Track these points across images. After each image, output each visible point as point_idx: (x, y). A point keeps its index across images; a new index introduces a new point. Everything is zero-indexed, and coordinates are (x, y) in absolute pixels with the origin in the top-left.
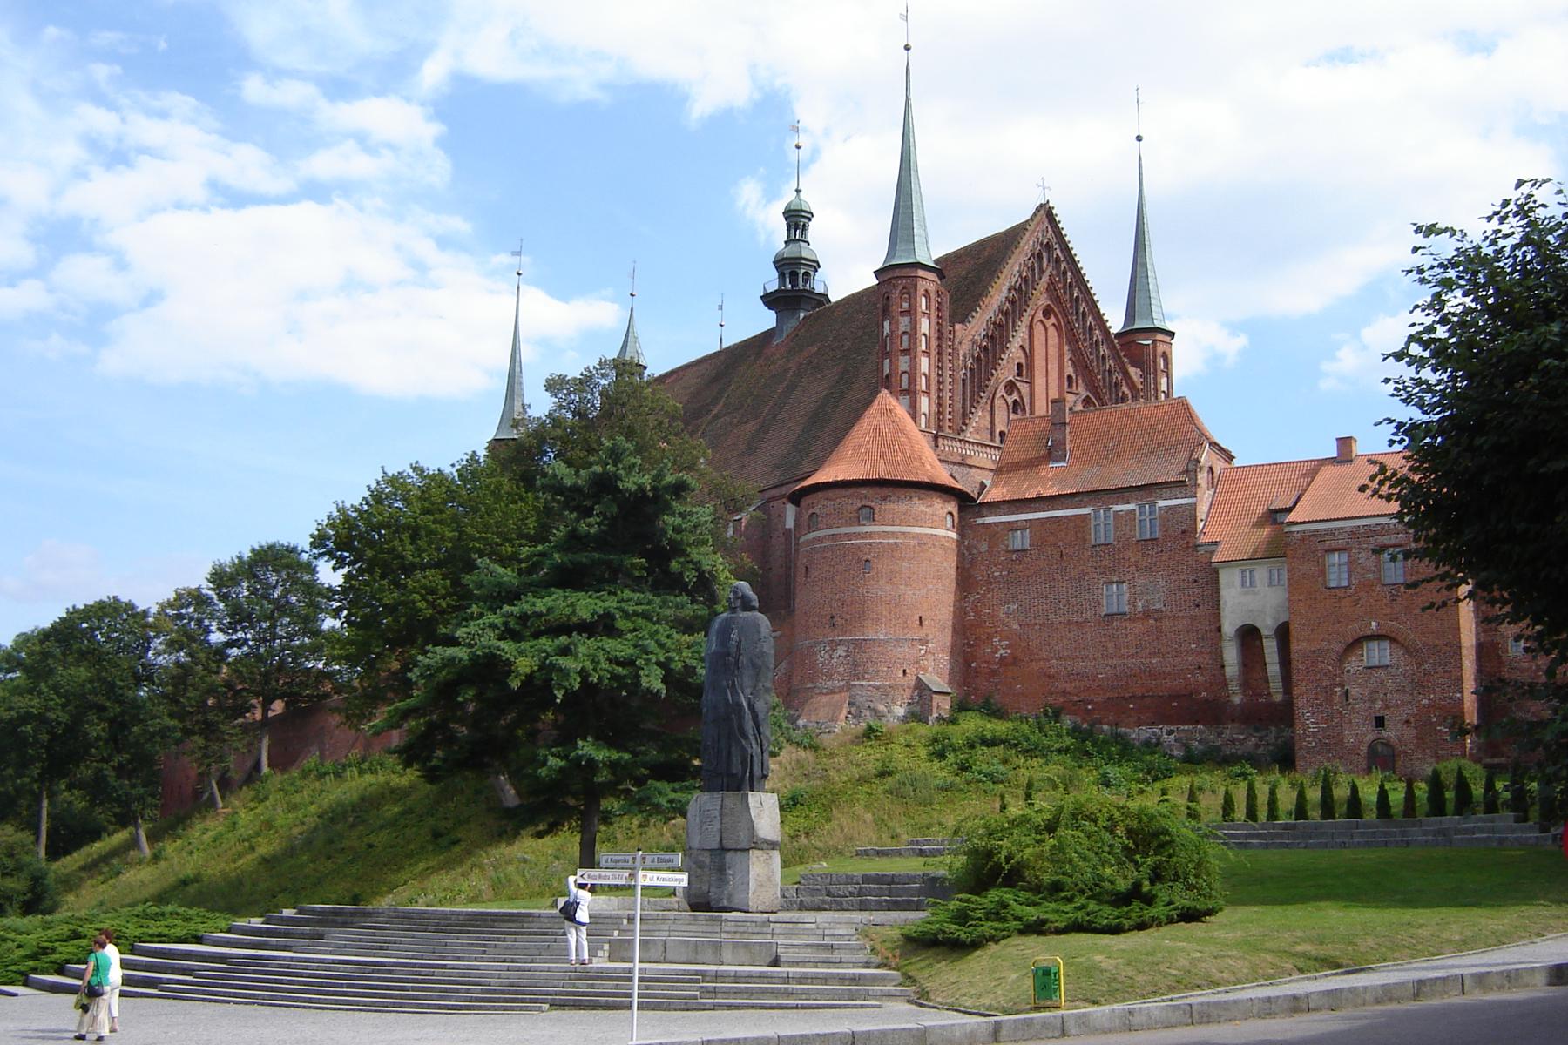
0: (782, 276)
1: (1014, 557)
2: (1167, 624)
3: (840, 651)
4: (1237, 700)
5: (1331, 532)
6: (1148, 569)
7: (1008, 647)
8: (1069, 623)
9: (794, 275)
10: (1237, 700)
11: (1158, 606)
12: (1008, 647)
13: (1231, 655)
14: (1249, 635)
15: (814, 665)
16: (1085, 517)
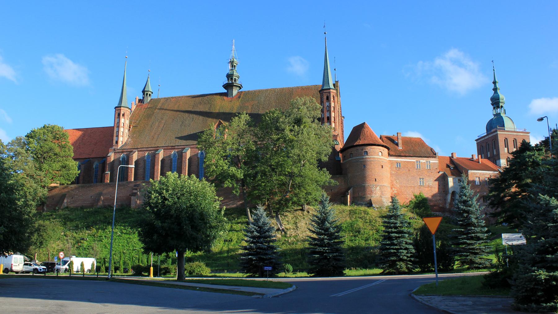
0: (228, 79)
1: (397, 169)
2: (433, 189)
3: (378, 188)
4: (448, 207)
5: (477, 173)
6: (429, 176)
7: (396, 191)
8: (411, 187)
9: (232, 79)
10: (448, 207)
11: (431, 185)
12: (396, 191)
13: (449, 197)
14: (454, 193)
15: (371, 191)
16: (414, 162)
